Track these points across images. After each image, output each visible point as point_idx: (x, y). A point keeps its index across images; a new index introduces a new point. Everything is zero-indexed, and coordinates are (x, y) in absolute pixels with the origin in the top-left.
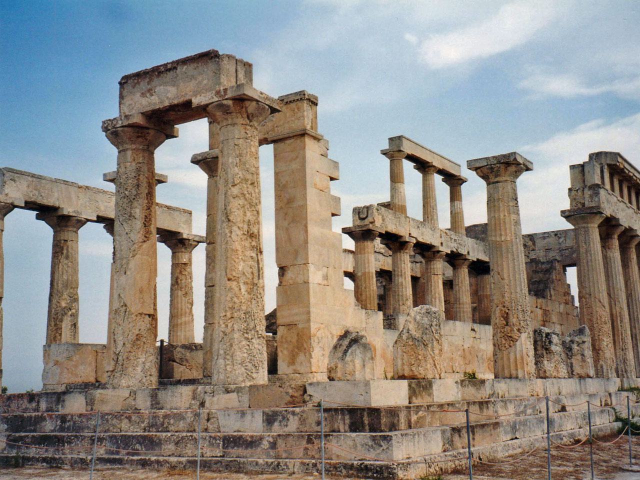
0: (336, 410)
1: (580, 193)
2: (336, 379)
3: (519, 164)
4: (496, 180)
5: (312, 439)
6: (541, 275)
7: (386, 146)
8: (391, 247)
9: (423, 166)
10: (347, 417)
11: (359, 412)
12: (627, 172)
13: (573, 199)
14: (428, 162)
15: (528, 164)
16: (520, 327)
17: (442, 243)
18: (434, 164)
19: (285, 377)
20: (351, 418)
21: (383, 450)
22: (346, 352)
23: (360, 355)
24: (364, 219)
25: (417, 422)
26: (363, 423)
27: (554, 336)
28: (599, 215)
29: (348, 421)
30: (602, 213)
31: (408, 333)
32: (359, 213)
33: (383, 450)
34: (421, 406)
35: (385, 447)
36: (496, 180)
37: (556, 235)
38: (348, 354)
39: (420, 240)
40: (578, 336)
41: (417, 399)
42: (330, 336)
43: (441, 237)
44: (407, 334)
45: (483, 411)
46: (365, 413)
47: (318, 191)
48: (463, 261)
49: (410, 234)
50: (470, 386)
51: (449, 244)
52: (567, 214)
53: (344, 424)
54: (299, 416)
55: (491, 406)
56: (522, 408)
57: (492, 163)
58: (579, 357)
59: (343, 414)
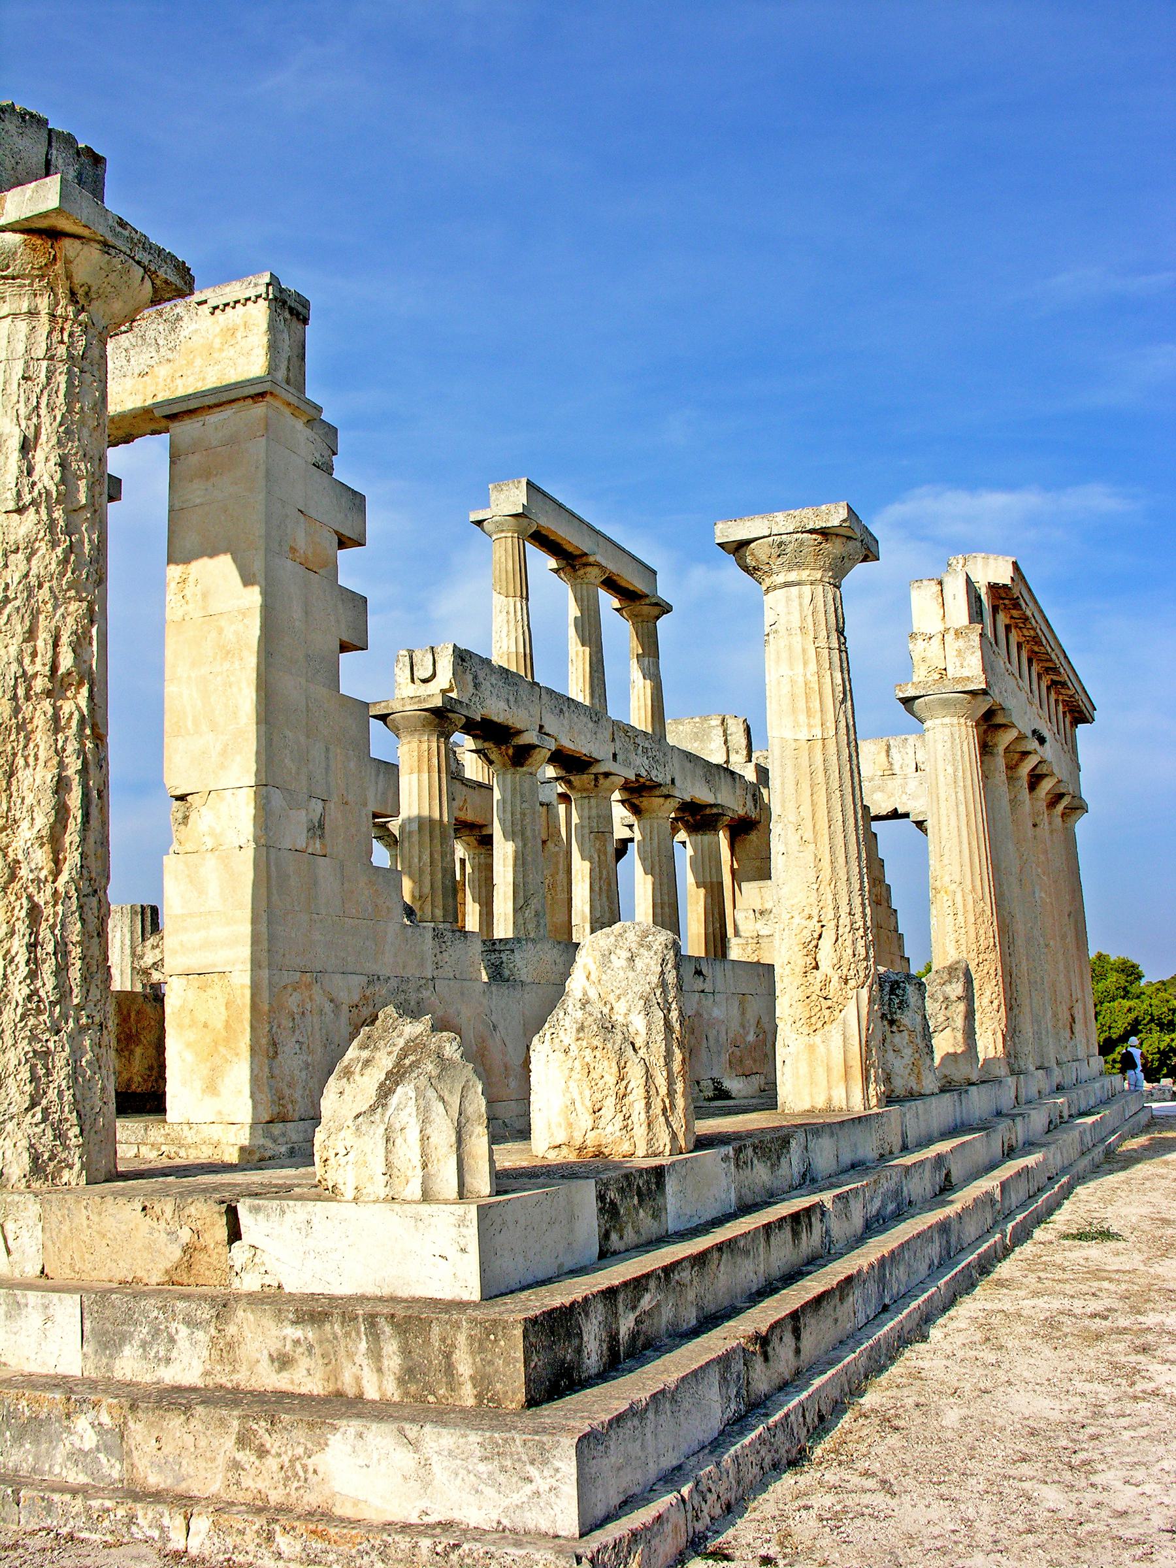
1: (937, 641)
2: (349, 1194)
8: (493, 757)
10: (391, 1348)
17: (615, 755)
18: (599, 558)
20: (406, 1352)
21: (537, 1493)
22: (385, 1092)
24: (425, 681)
25: (634, 1336)
26: (449, 1369)
28: (981, 698)
29: (393, 1361)
33: (537, 1493)
35: (542, 1484)
38: (394, 1100)
39: (567, 743)
42: (328, 1007)
43: (613, 740)
44: (579, 1014)
45: (799, 1239)
46: (462, 1339)
47: (301, 570)
48: (661, 800)
49: (541, 727)
51: (633, 756)
53: (380, 1370)
54: (213, 1332)
59: (374, 1335)
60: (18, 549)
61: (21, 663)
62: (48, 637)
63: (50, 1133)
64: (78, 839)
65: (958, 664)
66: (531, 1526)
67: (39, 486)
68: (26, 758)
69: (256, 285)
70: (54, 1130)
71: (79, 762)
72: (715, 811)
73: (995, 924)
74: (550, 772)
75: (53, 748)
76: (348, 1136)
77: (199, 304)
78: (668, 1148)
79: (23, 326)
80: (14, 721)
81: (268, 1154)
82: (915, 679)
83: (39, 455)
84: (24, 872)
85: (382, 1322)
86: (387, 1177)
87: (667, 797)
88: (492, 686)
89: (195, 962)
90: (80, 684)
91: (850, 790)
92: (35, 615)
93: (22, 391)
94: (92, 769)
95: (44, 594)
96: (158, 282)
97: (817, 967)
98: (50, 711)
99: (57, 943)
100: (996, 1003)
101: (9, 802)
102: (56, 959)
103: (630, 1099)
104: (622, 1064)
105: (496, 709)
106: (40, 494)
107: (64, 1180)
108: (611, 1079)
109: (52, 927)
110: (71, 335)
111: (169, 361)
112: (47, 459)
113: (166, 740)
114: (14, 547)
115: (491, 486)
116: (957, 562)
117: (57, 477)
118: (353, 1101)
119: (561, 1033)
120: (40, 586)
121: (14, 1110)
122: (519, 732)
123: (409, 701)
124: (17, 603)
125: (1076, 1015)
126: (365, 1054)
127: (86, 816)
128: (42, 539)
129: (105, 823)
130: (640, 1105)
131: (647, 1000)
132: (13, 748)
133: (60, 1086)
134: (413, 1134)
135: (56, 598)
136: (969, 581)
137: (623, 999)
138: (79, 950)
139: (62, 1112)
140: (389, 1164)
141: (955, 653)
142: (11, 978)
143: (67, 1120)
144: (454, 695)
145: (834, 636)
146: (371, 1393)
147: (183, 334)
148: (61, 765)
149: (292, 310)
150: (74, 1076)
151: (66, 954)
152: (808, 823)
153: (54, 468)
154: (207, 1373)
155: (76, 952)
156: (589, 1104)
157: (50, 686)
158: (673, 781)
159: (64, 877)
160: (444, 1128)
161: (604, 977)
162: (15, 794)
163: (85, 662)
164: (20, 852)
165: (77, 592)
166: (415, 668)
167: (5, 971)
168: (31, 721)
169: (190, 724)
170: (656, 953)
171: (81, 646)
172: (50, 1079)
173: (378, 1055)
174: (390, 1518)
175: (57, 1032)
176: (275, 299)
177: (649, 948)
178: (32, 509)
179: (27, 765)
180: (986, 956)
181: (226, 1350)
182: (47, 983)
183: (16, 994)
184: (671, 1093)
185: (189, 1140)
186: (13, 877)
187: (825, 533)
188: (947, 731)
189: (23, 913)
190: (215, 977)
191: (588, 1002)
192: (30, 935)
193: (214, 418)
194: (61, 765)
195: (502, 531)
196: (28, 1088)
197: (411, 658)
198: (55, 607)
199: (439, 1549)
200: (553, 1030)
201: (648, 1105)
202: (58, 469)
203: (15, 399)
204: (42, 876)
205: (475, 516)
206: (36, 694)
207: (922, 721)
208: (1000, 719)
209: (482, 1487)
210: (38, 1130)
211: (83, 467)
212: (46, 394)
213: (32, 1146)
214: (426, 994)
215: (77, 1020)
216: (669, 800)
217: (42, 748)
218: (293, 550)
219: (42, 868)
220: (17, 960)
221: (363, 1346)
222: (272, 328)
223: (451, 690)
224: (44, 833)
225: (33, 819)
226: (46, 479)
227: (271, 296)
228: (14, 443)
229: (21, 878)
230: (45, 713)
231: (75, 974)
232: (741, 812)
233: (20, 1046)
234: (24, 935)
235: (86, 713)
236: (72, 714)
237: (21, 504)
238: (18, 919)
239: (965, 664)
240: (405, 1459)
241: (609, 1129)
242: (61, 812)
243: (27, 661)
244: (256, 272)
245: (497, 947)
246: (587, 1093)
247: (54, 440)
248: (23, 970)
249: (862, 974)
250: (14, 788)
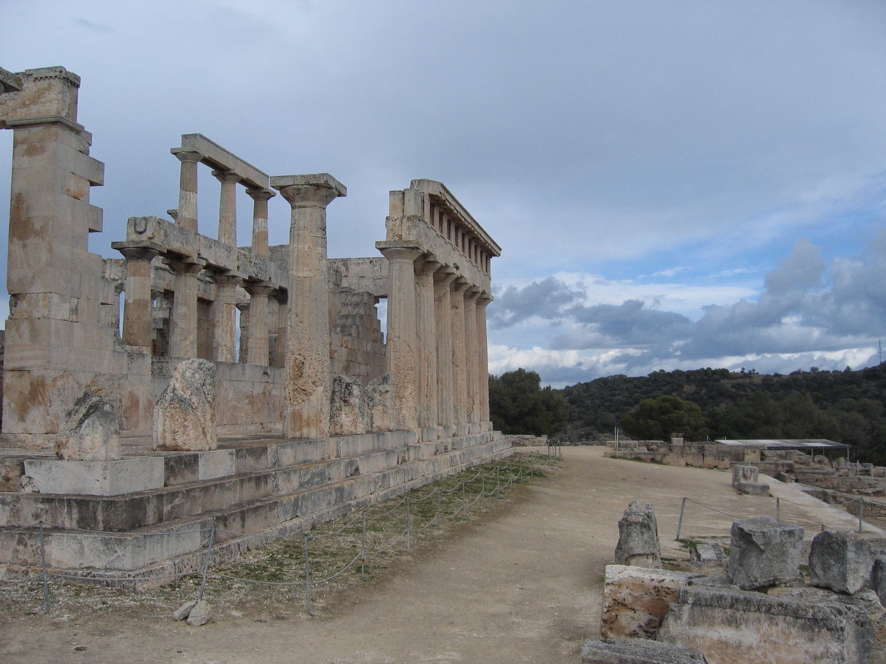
0: (61, 501)
1: (398, 222)
2: (66, 458)
3: (330, 188)
4: (303, 203)
5: (24, 539)
6: (350, 309)
7: (178, 144)
9: (222, 172)
10: (75, 511)
11: (91, 504)
12: (448, 204)
13: (390, 230)
14: (230, 169)
15: (341, 189)
16: (316, 380)
17: (238, 267)
18: (236, 172)
19: (11, 437)
20: (80, 512)
21: (118, 556)
22: (82, 422)
23: (100, 428)
24: (141, 233)
25: (170, 513)
26: (95, 518)
27: (354, 387)
28: (415, 251)
29: (76, 516)
30: (419, 249)
31: (173, 392)
32: (135, 225)
33: (118, 556)
34: (178, 492)
35: (120, 553)
36: (303, 203)
37: (371, 262)
38: (84, 425)
39: (212, 262)
40: (382, 385)
41: (175, 480)
42: (76, 386)
43: (238, 259)
44: (172, 394)
46: (100, 507)
48: (264, 288)
49: (199, 254)
50: (247, 456)
52: (382, 246)
53: (71, 519)
54: (11, 506)
55: (270, 481)
56: (308, 477)
58: (380, 408)
59: (70, 507)
66: (116, 567)
81: (45, 446)
85: (72, 502)
89: (17, 365)
111: (14, 99)
122: (188, 257)
123: (131, 243)
125: (475, 401)
146: (67, 525)
149: (71, 81)
154: (9, 521)
174: (69, 567)
181: (15, 513)
190: (26, 373)
191: (176, 390)
193: (34, 130)
199: (84, 574)
209: (101, 555)
214: (122, 381)
218: (68, 190)
221: (66, 510)
240: (75, 546)
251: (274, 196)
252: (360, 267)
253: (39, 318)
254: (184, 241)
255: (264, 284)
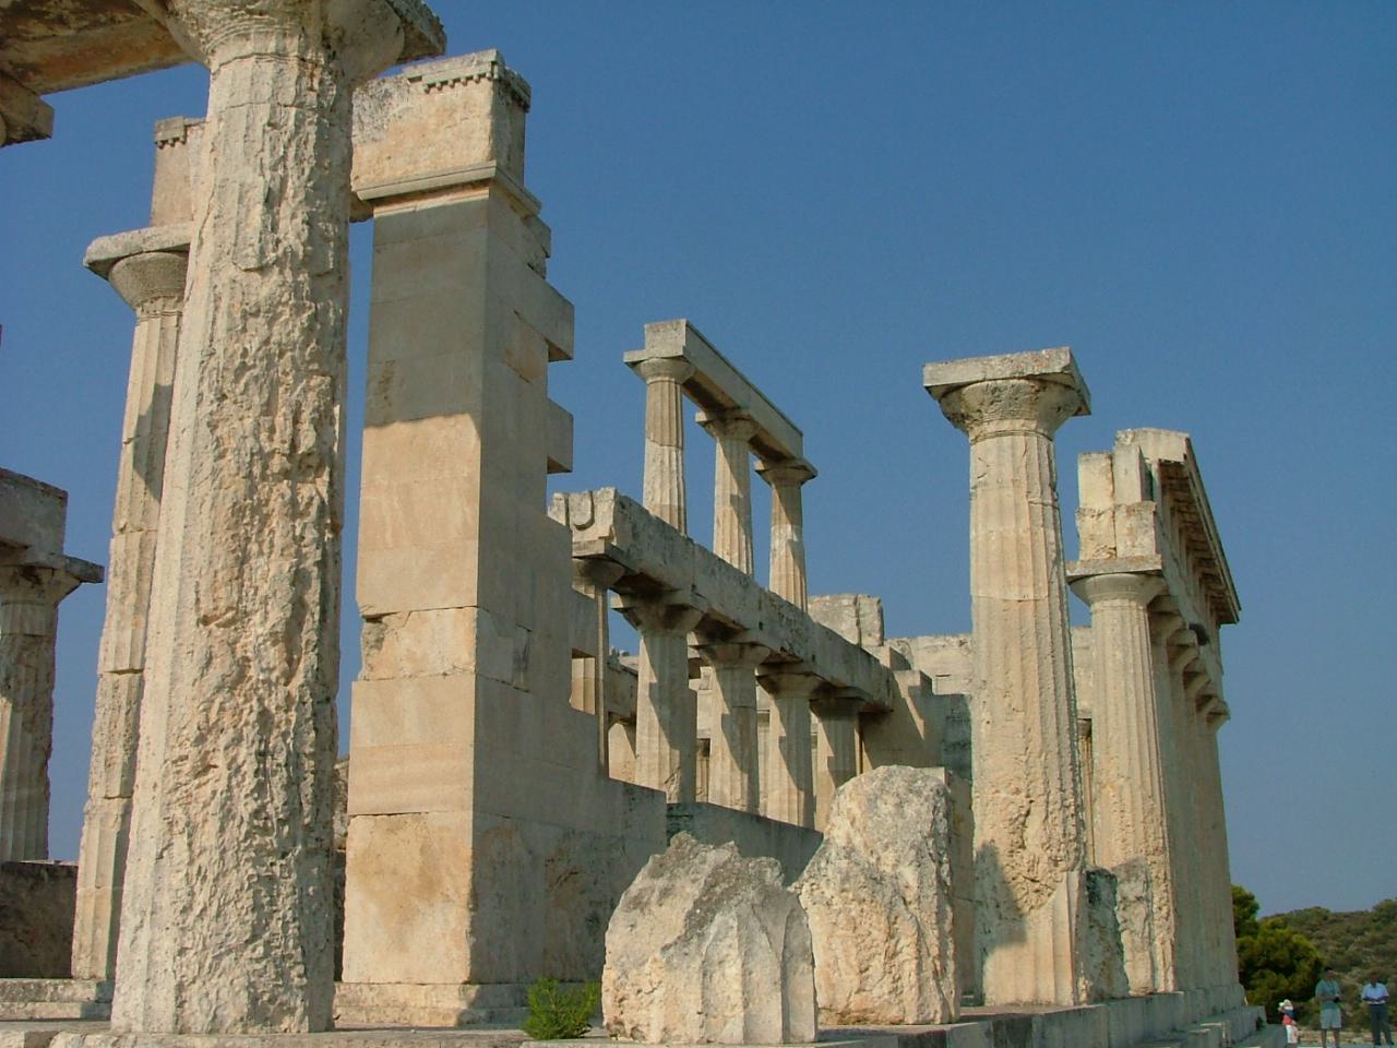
1: (1105, 519)
8: (641, 617)
17: (761, 624)
18: (752, 412)
22: (697, 921)
28: (1154, 580)
39: (716, 607)
43: (760, 608)
44: (844, 863)
49: (694, 587)
57: (999, 375)
60: (259, 311)
61: (257, 438)
62: (288, 412)
63: (271, 970)
64: (315, 638)
65: (1129, 543)
67: (285, 243)
68: (260, 544)
69: (479, 63)
70: (276, 967)
71: (319, 552)
72: (851, 694)
73: (1165, 824)
74: (692, 640)
75: (291, 535)
76: (651, 972)
77: (412, 80)
78: (938, 1016)
79: (269, 68)
80: (249, 501)
82: (1081, 558)
83: (285, 210)
84: (253, 672)
86: (703, 1017)
87: (808, 674)
88: (650, 537)
89: (384, 801)
90: (318, 470)
91: (1062, 656)
92: (274, 386)
93: (267, 137)
94: (330, 562)
95: (285, 363)
96: (411, 36)
97: (1023, 847)
98: (288, 493)
99: (289, 753)
100: (1165, 909)
101: (240, 592)
102: (288, 771)
103: (901, 958)
104: (892, 920)
105: (651, 561)
106: (285, 253)
107: (283, 1027)
108: (879, 935)
109: (285, 735)
110: (321, 82)
111: (374, 140)
112: (294, 216)
113: (360, 554)
114: (254, 310)
115: (646, 326)
116: (1126, 436)
117: (305, 235)
118: (651, 934)
119: (823, 884)
120: (281, 355)
121: (233, 942)
122: (673, 591)
124: (255, 372)
126: (661, 883)
127: (323, 612)
128: (287, 303)
129: (336, 626)
130: (911, 966)
131: (919, 850)
132: (246, 531)
133: (284, 917)
134: (733, 970)
135: (298, 370)
136: (1141, 457)
137: (890, 849)
138: (312, 763)
139: (286, 947)
140: (705, 1002)
141: (1125, 531)
142: (236, 791)
143: (290, 956)
144: (614, 543)
145: (1048, 491)
147: (391, 112)
148: (300, 556)
149: (514, 94)
150: (298, 908)
151: (298, 766)
152: (1017, 690)
153: (301, 226)
155: (309, 764)
156: (854, 963)
157: (288, 465)
158: (814, 657)
159: (299, 679)
160: (768, 962)
161: (870, 824)
162: (247, 583)
163: (325, 443)
164: (250, 648)
165: (320, 366)
166: (571, 513)
167: (230, 782)
168: (267, 505)
169: (388, 536)
170: (926, 800)
171: (322, 425)
172: (274, 908)
173: (678, 883)
175: (284, 856)
176: (500, 80)
177: (919, 793)
178: (276, 269)
179: (261, 553)
180: (1155, 858)
182: (277, 800)
183: (241, 807)
184: (942, 956)
185: (369, 1002)
186: (242, 676)
187: (1042, 381)
188: (1117, 614)
189: (253, 717)
191: (853, 850)
192: (260, 742)
194: (300, 556)
195: (659, 375)
196: (250, 917)
197: (567, 501)
198: (297, 380)
200: (813, 881)
201: (919, 967)
202: (306, 227)
203: (258, 146)
204: (273, 676)
205: (629, 357)
206: (273, 474)
207: (1089, 603)
208: (1166, 606)
210: (258, 966)
211: (330, 228)
212: (294, 144)
213: (251, 985)
215: (305, 844)
216: (810, 679)
217: (277, 534)
218: (508, 352)
219: (274, 668)
220: (244, 768)
222: (495, 112)
223: (610, 538)
224: (278, 629)
225: (266, 612)
226: (291, 237)
227: (496, 76)
228: (258, 194)
229: (250, 678)
230: (283, 496)
231: (307, 789)
232: (876, 699)
233: (243, 869)
234: (253, 742)
235: (326, 500)
236: (312, 499)
237: (264, 262)
238: (247, 724)
239: (1136, 544)
241: (876, 992)
242: (299, 606)
243: (264, 436)
244: (480, 47)
245: (675, 812)
246: (854, 951)
247: (301, 196)
248: (250, 782)
249: (1072, 856)
250: (246, 576)
251: (814, 477)
252: (938, 655)
253: (445, 674)
254: (667, 553)
255: (805, 668)
